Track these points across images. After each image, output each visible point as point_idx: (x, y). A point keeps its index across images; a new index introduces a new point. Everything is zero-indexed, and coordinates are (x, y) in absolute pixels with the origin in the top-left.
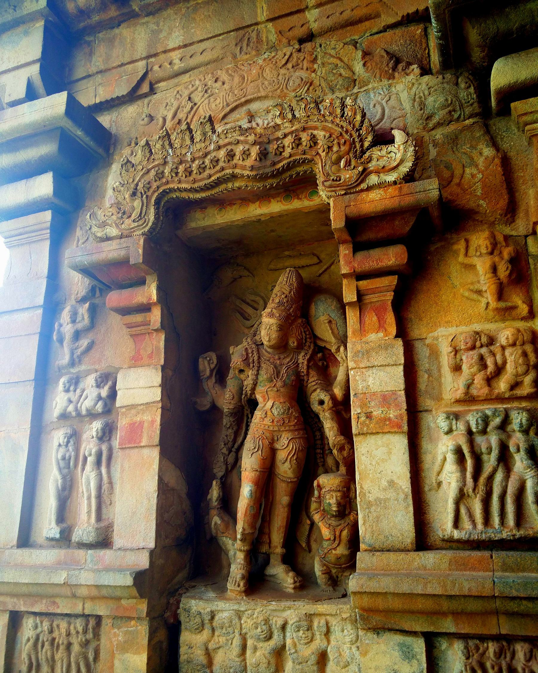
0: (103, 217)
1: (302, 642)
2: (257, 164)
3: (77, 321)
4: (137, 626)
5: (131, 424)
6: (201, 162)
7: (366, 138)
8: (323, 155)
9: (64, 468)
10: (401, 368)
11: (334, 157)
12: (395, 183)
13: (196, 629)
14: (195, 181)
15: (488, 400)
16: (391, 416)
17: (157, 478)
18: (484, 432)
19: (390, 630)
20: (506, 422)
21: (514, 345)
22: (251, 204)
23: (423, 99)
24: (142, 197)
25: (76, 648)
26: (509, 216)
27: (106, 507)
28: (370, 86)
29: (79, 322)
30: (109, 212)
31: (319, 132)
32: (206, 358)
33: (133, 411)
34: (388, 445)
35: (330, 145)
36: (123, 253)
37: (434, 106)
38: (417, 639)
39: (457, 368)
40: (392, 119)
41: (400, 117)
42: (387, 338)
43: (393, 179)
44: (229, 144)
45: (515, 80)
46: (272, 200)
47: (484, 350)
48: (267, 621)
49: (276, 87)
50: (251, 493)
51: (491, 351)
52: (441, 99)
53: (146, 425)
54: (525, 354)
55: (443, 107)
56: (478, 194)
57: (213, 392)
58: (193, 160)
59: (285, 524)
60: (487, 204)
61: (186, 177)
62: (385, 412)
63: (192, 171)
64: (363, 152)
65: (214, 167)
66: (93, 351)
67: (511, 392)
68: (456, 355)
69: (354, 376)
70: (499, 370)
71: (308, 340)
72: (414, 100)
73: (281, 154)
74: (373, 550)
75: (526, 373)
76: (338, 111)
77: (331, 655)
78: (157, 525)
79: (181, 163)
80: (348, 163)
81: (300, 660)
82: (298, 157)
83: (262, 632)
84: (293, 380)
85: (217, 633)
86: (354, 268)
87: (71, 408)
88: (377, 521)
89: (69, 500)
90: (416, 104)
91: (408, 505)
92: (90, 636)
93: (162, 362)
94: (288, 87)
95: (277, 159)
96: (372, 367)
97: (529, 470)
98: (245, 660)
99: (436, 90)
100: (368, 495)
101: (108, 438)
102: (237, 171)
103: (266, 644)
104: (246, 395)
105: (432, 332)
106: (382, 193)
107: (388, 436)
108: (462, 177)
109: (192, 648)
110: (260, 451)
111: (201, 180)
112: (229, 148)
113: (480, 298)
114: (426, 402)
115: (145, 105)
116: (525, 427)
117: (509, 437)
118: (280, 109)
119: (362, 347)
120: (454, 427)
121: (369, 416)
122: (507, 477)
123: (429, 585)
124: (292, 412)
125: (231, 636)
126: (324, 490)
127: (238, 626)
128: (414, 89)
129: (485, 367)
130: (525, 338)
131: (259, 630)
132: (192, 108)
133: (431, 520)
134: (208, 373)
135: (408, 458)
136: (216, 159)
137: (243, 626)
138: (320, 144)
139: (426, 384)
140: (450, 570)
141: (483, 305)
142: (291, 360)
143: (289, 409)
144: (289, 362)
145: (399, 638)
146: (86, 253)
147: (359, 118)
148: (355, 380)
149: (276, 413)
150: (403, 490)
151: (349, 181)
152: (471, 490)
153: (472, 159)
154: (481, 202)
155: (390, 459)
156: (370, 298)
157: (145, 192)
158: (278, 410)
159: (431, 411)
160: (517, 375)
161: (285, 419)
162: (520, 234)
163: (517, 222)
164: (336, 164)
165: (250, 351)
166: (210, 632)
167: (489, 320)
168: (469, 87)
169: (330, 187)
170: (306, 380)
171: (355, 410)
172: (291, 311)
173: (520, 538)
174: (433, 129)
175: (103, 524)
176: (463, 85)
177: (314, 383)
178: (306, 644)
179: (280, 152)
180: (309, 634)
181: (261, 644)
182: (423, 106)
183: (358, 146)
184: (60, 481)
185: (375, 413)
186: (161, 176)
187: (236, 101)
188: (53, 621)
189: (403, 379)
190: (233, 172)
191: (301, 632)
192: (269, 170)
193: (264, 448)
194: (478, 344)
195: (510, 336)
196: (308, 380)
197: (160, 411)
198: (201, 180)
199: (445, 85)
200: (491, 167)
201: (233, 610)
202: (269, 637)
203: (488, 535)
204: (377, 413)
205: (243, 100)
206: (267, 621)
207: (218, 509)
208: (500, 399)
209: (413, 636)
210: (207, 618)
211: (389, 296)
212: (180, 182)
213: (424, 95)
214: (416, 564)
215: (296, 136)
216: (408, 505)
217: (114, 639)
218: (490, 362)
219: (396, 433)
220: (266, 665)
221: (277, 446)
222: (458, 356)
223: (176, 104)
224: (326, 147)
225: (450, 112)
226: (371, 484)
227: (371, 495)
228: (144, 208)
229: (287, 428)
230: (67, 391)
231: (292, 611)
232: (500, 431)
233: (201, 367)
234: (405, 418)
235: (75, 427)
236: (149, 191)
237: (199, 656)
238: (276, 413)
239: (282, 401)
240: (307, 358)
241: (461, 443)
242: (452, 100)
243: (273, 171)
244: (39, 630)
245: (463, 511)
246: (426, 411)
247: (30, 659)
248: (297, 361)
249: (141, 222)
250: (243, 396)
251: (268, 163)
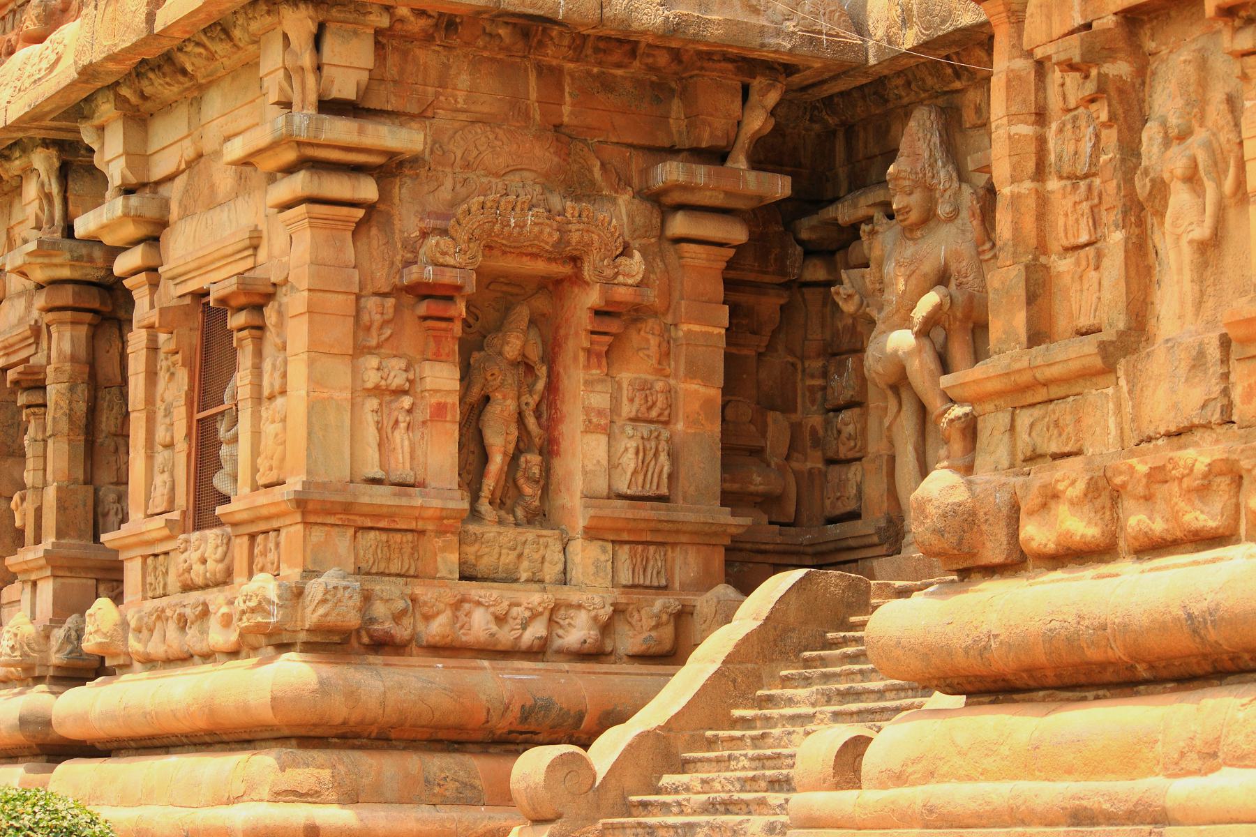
47: (648, 392)
53: (449, 406)
70: (654, 404)
77: (548, 557)
107: (599, 435)
122: (656, 464)
126: (529, 465)
129: (647, 401)
145: (601, 543)
202: (515, 549)
204: (595, 420)
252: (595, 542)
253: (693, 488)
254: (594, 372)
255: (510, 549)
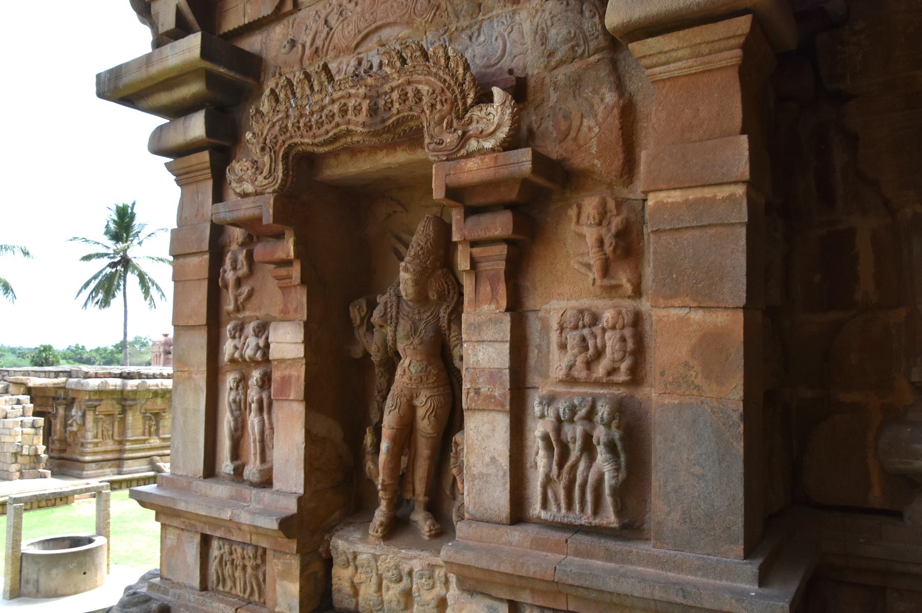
0: (240, 172)
1: (425, 588)
2: (369, 121)
3: (238, 268)
4: (291, 560)
5: (282, 377)
6: (319, 117)
7: (469, 94)
8: (428, 112)
9: (236, 410)
10: (507, 345)
11: (437, 117)
12: (493, 150)
13: (343, 565)
14: (315, 137)
15: (588, 383)
16: (496, 394)
17: (303, 431)
18: (571, 421)
19: (482, 593)
20: (592, 412)
21: (614, 328)
22: (378, 152)
23: (545, 31)
24: (271, 151)
25: (249, 570)
26: (625, 177)
27: (270, 450)
28: (494, 13)
29: (240, 269)
30: (245, 166)
31: (423, 86)
32: (355, 306)
33: (283, 365)
34: (492, 423)
35: (433, 102)
36: (257, 212)
37: (556, 40)
38: (502, 604)
39: (563, 347)
40: (512, 56)
41: (520, 54)
42: (498, 311)
43: (491, 146)
44: (342, 97)
45: (628, 19)
46: (398, 149)
47: (586, 332)
48: (397, 567)
49: (404, 11)
50: (388, 450)
51: (592, 333)
52: (564, 31)
53: (293, 379)
54: (623, 339)
55: (566, 41)
56: (593, 152)
57: (364, 340)
58: (312, 113)
59: (426, 474)
60: (601, 164)
61: (307, 131)
62: (491, 390)
63: (312, 125)
64: (466, 111)
65: (331, 122)
66: (253, 298)
67: (608, 378)
68: (561, 333)
69: (467, 349)
70: (599, 354)
71: (451, 291)
72: (536, 33)
73: (390, 109)
74: (475, 519)
75: (622, 359)
76: (442, 61)
78: (305, 473)
79: (301, 116)
80: (450, 125)
81: (422, 603)
82: (406, 114)
83: (393, 575)
84: (431, 337)
85: (359, 571)
86: (465, 236)
87: (237, 355)
88: (479, 494)
89: (243, 439)
90: (537, 37)
91: (506, 482)
92: (259, 561)
93: (305, 318)
94: (416, 11)
95: (386, 116)
96: (483, 341)
97: (606, 464)
98: (381, 595)
99: (559, 20)
100: (473, 468)
101: (268, 387)
102: (351, 127)
103: (397, 586)
104: (391, 348)
105: (544, 304)
106: (479, 162)
107: (492, 414)
108: (579, 130)
109: (341, 580)
110: (397, 410)
111: (321, 135)
112: (343, 101)
113: (588, 272)
114: (534, 379)
115: (291, 25)
116: (605, 421)
117: (593, 428)
118: (388, 57)
119: (474, 320)
120: (546, 413)
121: (477, 391)
122: (589, 467)
123: (502, 564)
124: (430, 370)
125: (370, 575)
127: (375, 566)
128: (537, 18)
129: (587, 349)
130: (626, 321)
131: (390, 573)
132: (328, 34)
133: (530, 496)
134: (358, 321)
135: (509, 437)
136: (331, 113)
137: (379, 568)
138: (424, 102)
139: (535, 360)
140: (531, 549)
141: (591, 281)
142: (432, 314)
143: (427, 367)
144: (428, 317)
145: (489, 602)
146: (227, 210)
147: (461, 70)
148: (468, 353)
149: (413, 371)
150: (502, 467)
151: (450, 146)
152: (555, 477)
153: (592, 106)
154: (596, 161)
155: (494, 436)
156: (484, 266)
157: (273, 147)
158: (416, 368)
159: (538, 388)
160: (614, 361)
161: (423, 378)
162: (637, 198)
163: (635, 183)
164: (439, 125)
165: (389, 305)
166: (354, 569)
167: (597, 296)
168: (594, 16)
169: (434, 150)
170: (447, 334)
171: (466, 385)
172: (428, 263)
173: (596, 527)
174: (555, 68)
175: (266, 466)
176: (587, 14)
177: (454, 339)
178: (428, 590)
179: (388, 107)
180: (431, 582)
181: (392, 585)
182: (544, 40)
183: (460, 104)
184: (232, 423)
185: (482, 390)
186: (285, 130)
187: (367, 27)
188: (232, 545)
189: (508, 356)
190: (347, 128)
191: (424, 580)
192: (379, 127)
193: (401, 406)
194: (580, 324)
195: (610, 319)
196: (450, 334)
197: (304, 366)
198: (321, 135)
199: (569, 13)
200: (609, 119)
201: (370, 553)
202: (400, 580)
203: (570, 519)
205: (373, 26)
206: (397, 567)
207: (372, 454)
208: (598, 383)
209: (499, 601)
210: (351, 557)
211: (502, 266)
212: (302, 137)
213: (547, 26)
214: (504, 539)
215: (402, 90)
216: (506, 482)
217: (275, 568)
218: (591, 343)
219: (499, 411)
220: (396, 603)
221: (417, 403)
222: (563, 334)
223: (314, 26)
224: (429, 104)
225: (573, 47)
226: (476, 459)
227: (475, 469)
228: (273, 164)
229: (425, 386)
230: (234, 337)
231: (418, 560)
232: (585, 422)
233: (352, 315)
234: (508, 397)
235: (244, 371)
236: (276, 145)
237: (347, 588)
238: (413, 371)
239: (419, 358)
240: (448, 311)
241: (548, 431)
242: (575, 33)
243: (384, 128)
244: (222, 551)
245: (550, 494)
246: (534, 388)
247: (217, 573)
248: (439, 314)
249: (271, 180)
250: (389, 349)
251: (379, 119)
252: (478, 598)
253: (676, 515)
254: (485, 308)
255: (391, 581)
